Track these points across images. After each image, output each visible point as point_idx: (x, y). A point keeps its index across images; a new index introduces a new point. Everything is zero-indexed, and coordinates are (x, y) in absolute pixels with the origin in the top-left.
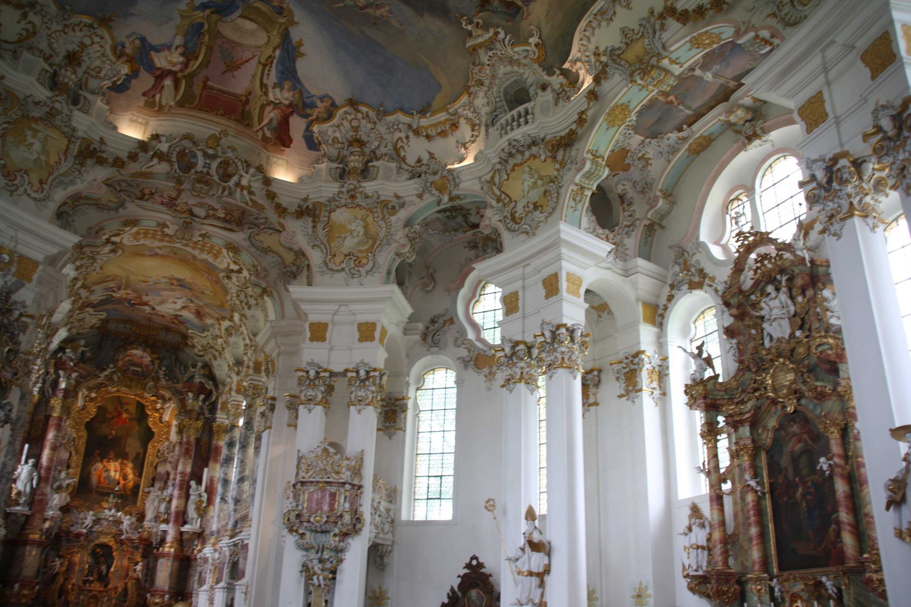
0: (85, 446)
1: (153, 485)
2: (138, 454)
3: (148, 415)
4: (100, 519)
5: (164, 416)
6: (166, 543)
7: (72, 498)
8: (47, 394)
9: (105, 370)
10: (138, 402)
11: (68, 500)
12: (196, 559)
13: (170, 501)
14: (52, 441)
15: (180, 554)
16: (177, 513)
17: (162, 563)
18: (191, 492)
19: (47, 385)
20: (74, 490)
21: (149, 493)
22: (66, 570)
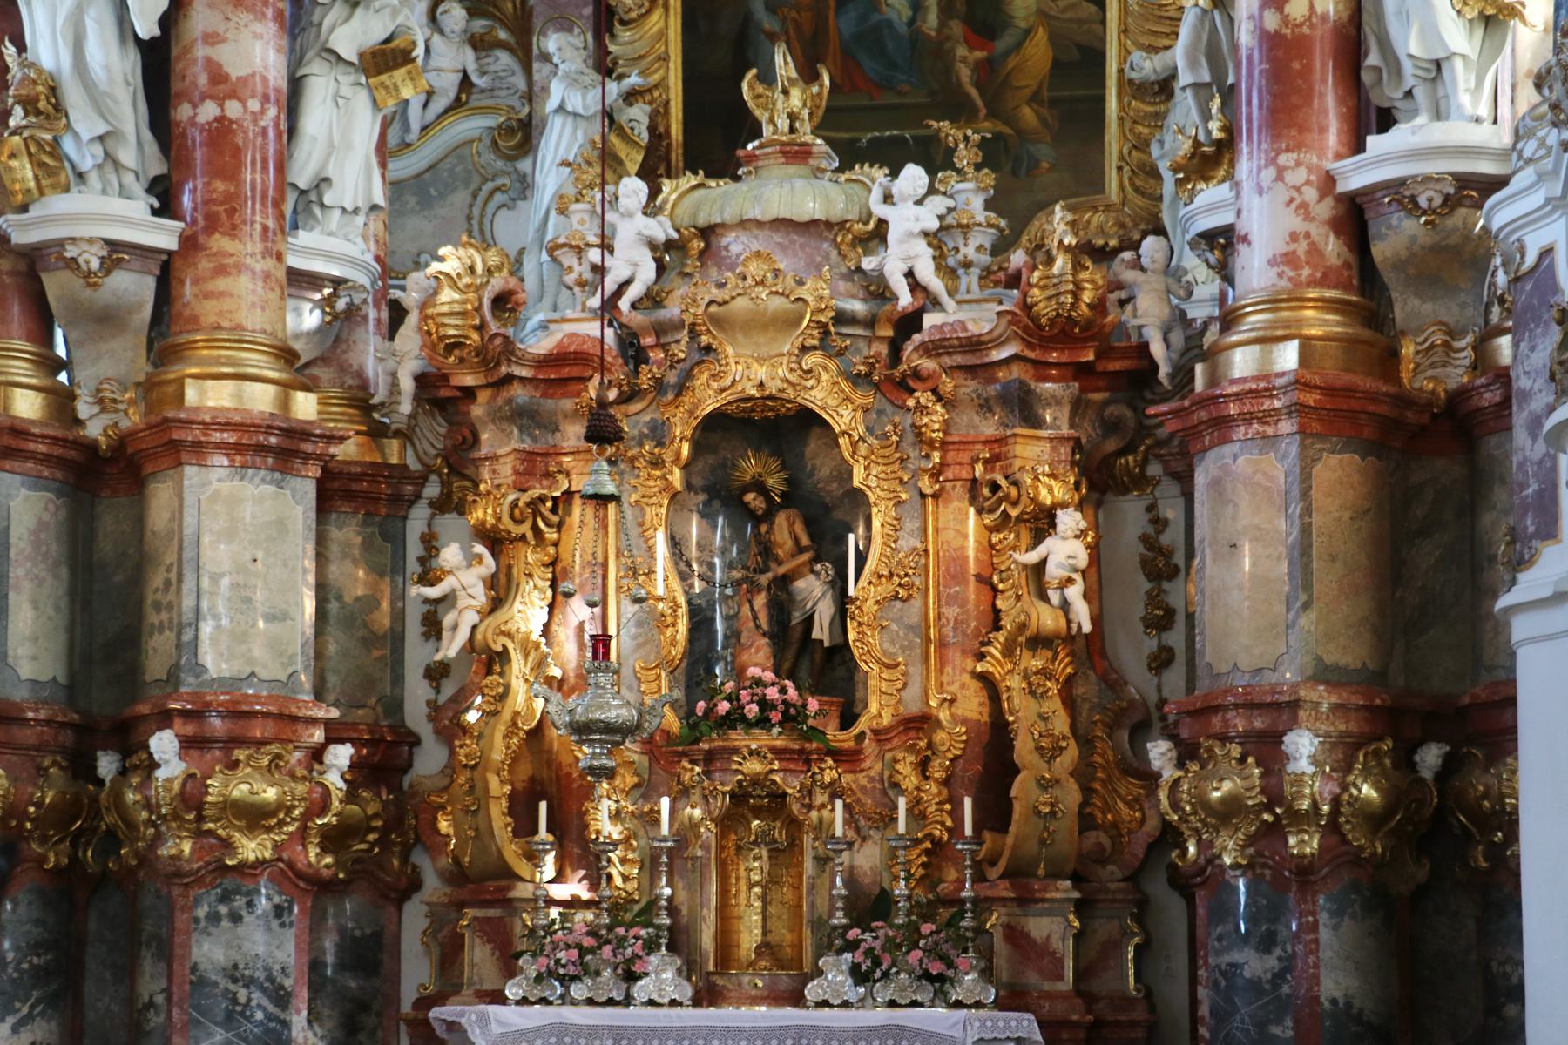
4: (708, 232)
15: (1367, 383)
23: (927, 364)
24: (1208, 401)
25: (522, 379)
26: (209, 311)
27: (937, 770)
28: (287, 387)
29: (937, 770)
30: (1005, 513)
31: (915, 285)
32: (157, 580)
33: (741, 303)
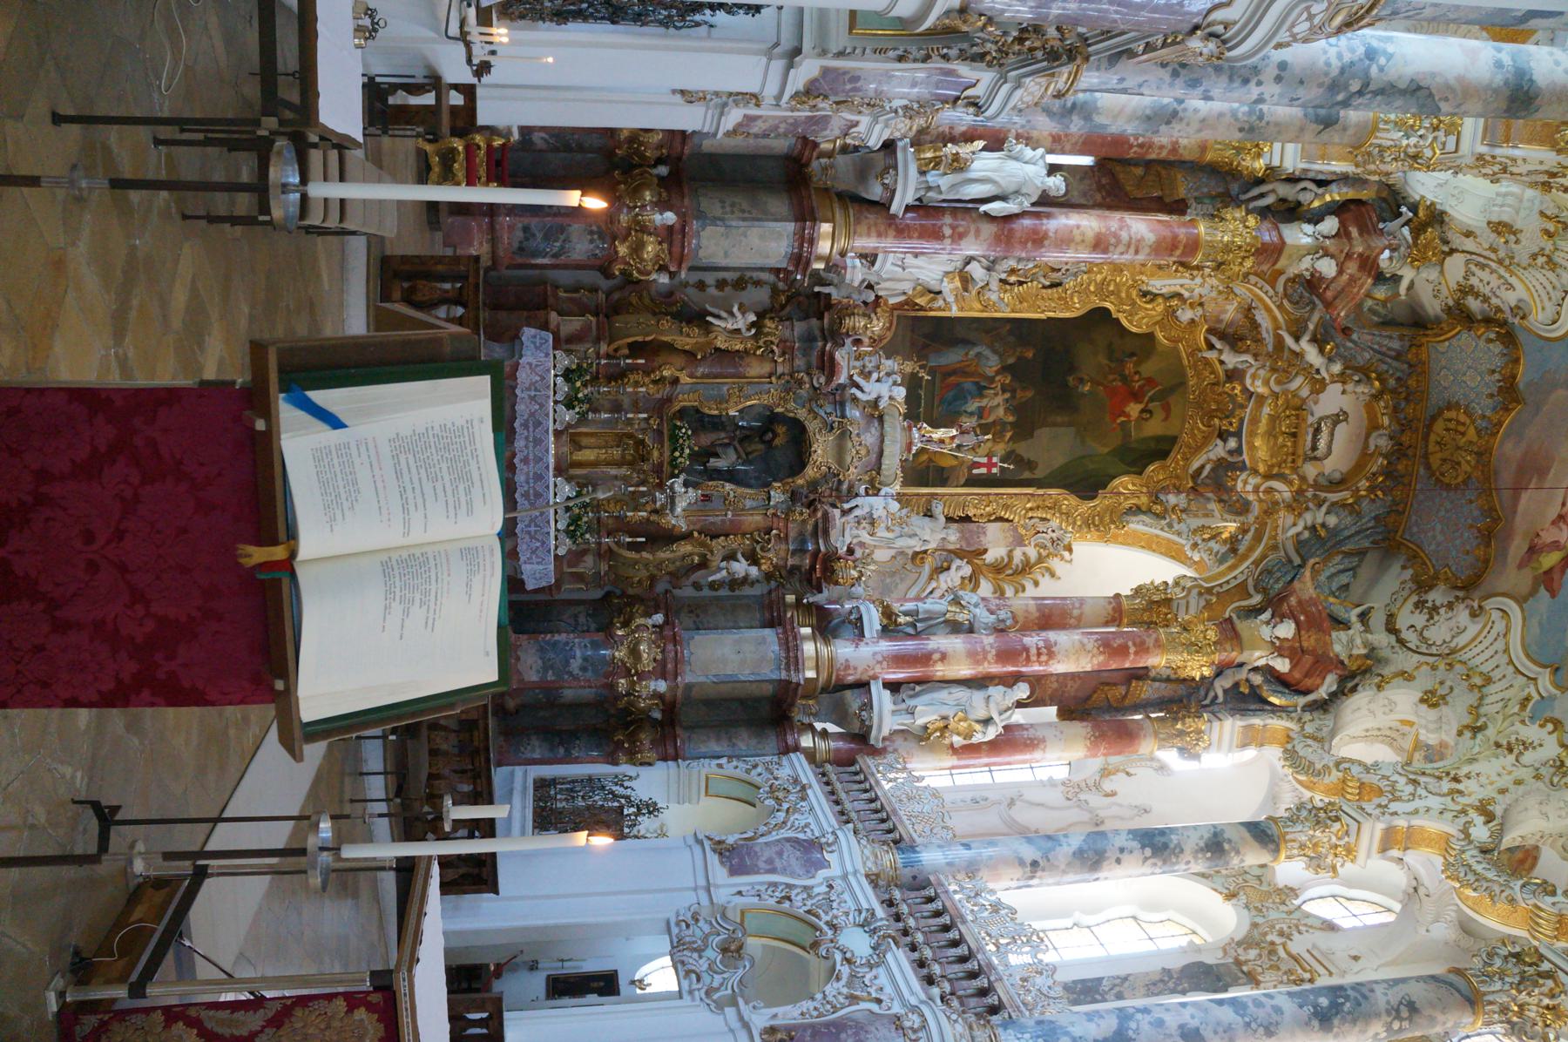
0: (1042, 316)
1: (949, 519)
2: (1031, 465)
3: (1140, 473)
4: (881, 419)
5: (1144, 518)
6: (827, 642)
7: (899, 306)
8: (1255, 192)
9: (1321, 351)
10: (1173, 440)
11: (892, 301)
12: (786, 750)
13: (955, 627)
14: (1124, 235)
16: (925, 659)
17: (763, 641)
18: (996, 691)
19: (1285, 191)
20: (922, 309)
21: (929, 514)
22: (717, 349)
23: (819, 514)
24: (795, 638)
25: (825, 345)
26: (862, 228)
27: (654, 518)
28: (827, 259)
29: (654, 518)
30: (758, 542)
31: (851, 509)
32: (745, 206)
33: (850, 444)
